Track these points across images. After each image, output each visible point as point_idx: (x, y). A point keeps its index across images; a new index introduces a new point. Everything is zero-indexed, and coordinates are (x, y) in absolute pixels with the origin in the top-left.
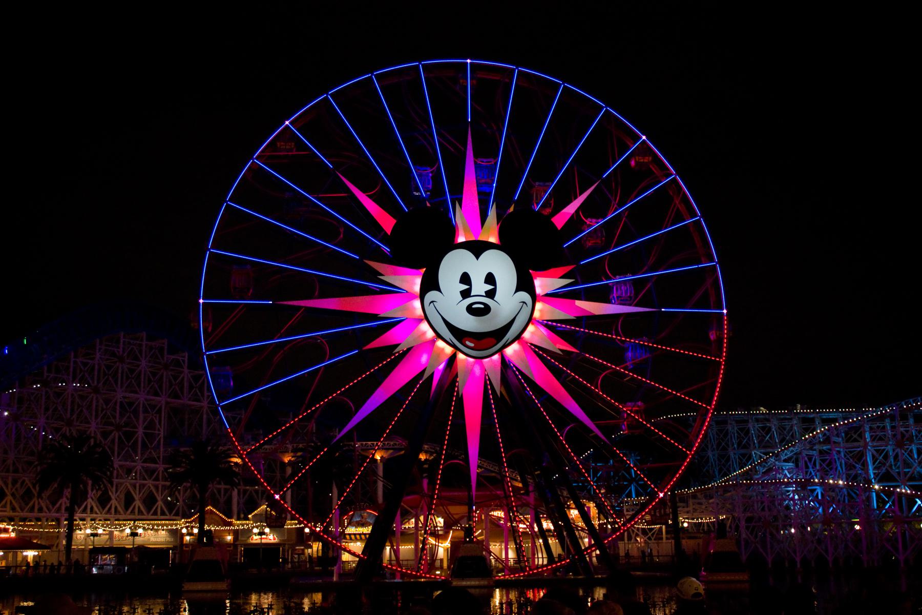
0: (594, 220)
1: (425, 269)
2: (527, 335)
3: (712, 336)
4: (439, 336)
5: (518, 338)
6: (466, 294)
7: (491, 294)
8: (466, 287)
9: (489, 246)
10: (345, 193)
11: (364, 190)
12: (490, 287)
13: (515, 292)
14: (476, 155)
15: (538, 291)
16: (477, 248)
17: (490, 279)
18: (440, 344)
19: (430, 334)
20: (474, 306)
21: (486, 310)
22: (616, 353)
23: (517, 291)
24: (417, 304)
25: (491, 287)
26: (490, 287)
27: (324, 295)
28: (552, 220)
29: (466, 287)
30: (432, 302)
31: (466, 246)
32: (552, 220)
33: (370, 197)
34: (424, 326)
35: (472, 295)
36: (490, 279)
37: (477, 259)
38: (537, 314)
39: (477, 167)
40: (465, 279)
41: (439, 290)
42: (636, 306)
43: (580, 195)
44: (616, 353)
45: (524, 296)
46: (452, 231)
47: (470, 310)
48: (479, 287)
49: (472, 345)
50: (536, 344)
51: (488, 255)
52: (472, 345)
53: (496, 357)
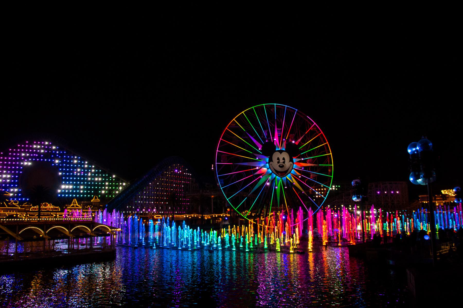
0: (304, 143)
1: (269, 157)
2: (292, 172)
3: (329, 171)
4: (273, 172)
5: (290, 173)
6: (278, 162)
7: (284, 162)
8: (278, 161)
9: (283, 151)
10: (247, 136)
11: (252, 136)
12: (284, 161)
14: (278, 127)
15: (294, 161)
16: (281, 152)
18: (273, 173)
19: (271, 172)
20: (281, 165)
22: (308, 175)
23: (290, 161)
24: (268, 165)
26: (284, 161)
27: (243, 162)
28: (297, 144)
29: (278, 161)
30: (271, 164)
31: (278, 151)
32: (297, 144)
33: (254, 138)
34: (269, 170)
35: (280, 162)
36: (284, 159)
37: (281, 153)
38: (294, 167)
39: (278, 130)
41: (273, 162)
42: (314, 164)
43: (301, 137)
44: (308, 175)
45: (291, 163)
46: (275, 148)
47: (279, 166)
49: (280, 174)
50: (293, 174)
51: (283, 153)
52: (280, 174)
53: (285, 177)
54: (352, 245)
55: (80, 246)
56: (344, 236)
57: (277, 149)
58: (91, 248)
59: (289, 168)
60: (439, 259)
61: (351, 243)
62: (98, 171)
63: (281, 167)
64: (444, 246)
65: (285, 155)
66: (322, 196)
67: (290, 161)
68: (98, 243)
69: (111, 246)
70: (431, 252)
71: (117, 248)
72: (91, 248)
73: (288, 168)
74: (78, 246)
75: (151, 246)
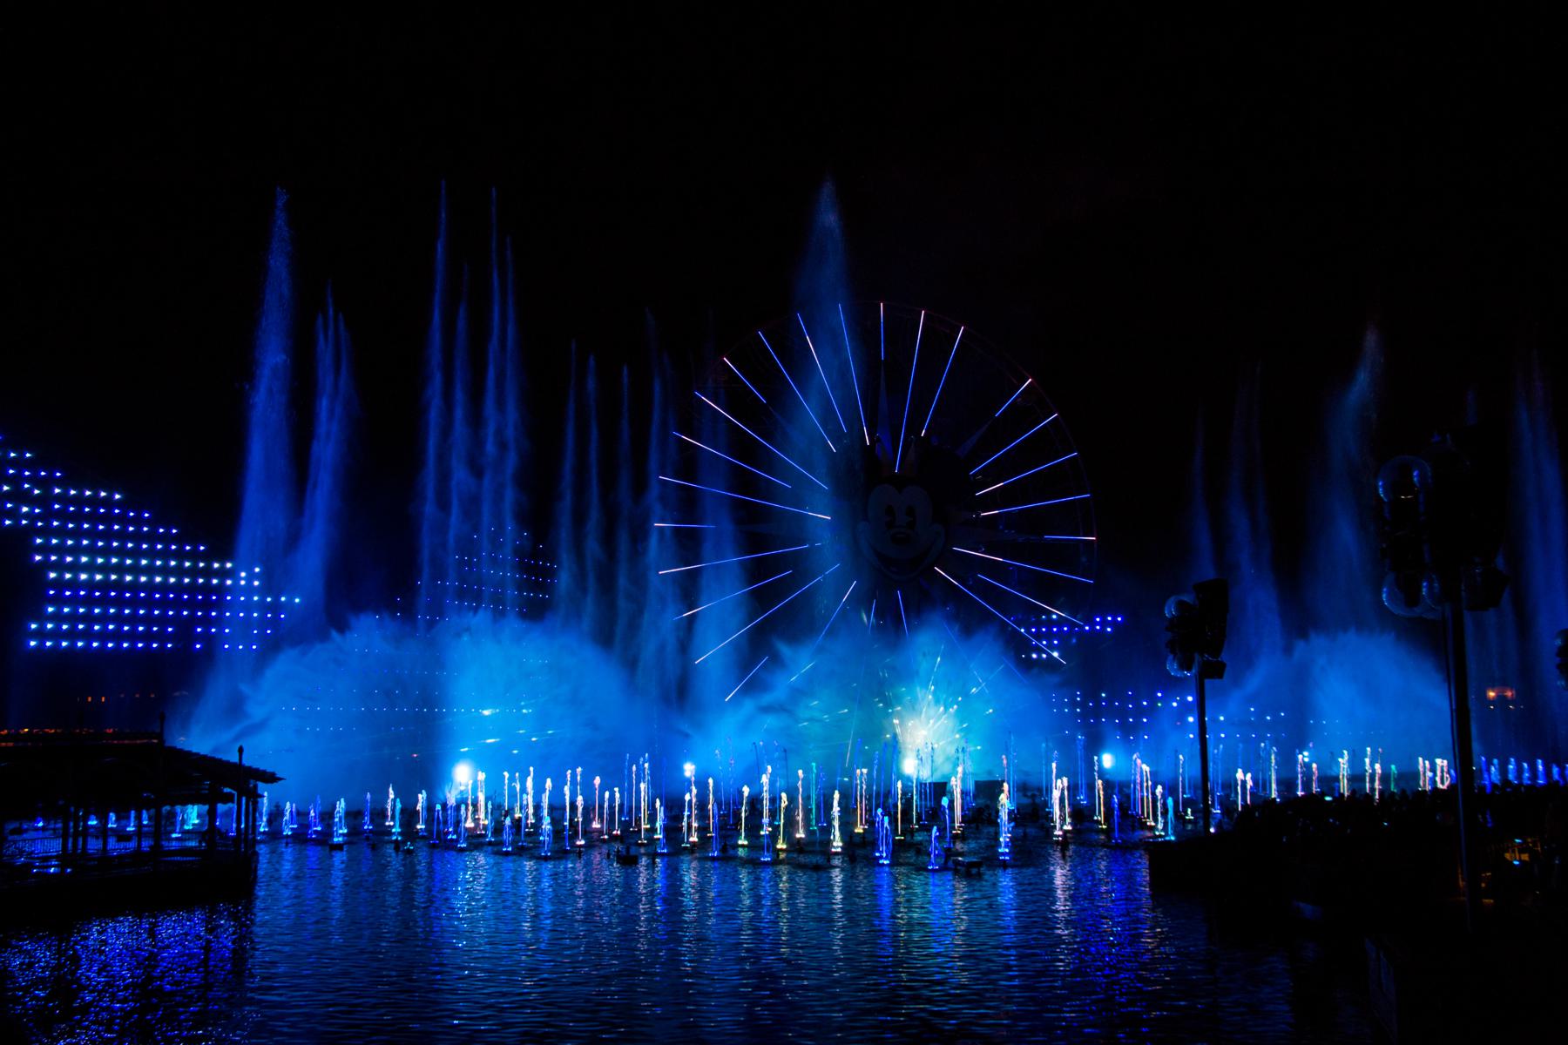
54: (1162, 842)
55: (112, 843)
56: (1132, 808)
58: (157, 848)
60: (1492, 901)
61: (1160, 836)
62: (195, 549)
64: (1514, 852)
66: (1055, 654)
68: (186, 827)
69: (236, 840)
70: (1460, 876)
71: (262, 850)
72: (157, 848)
74: (105, 844)
75: (397, 839)
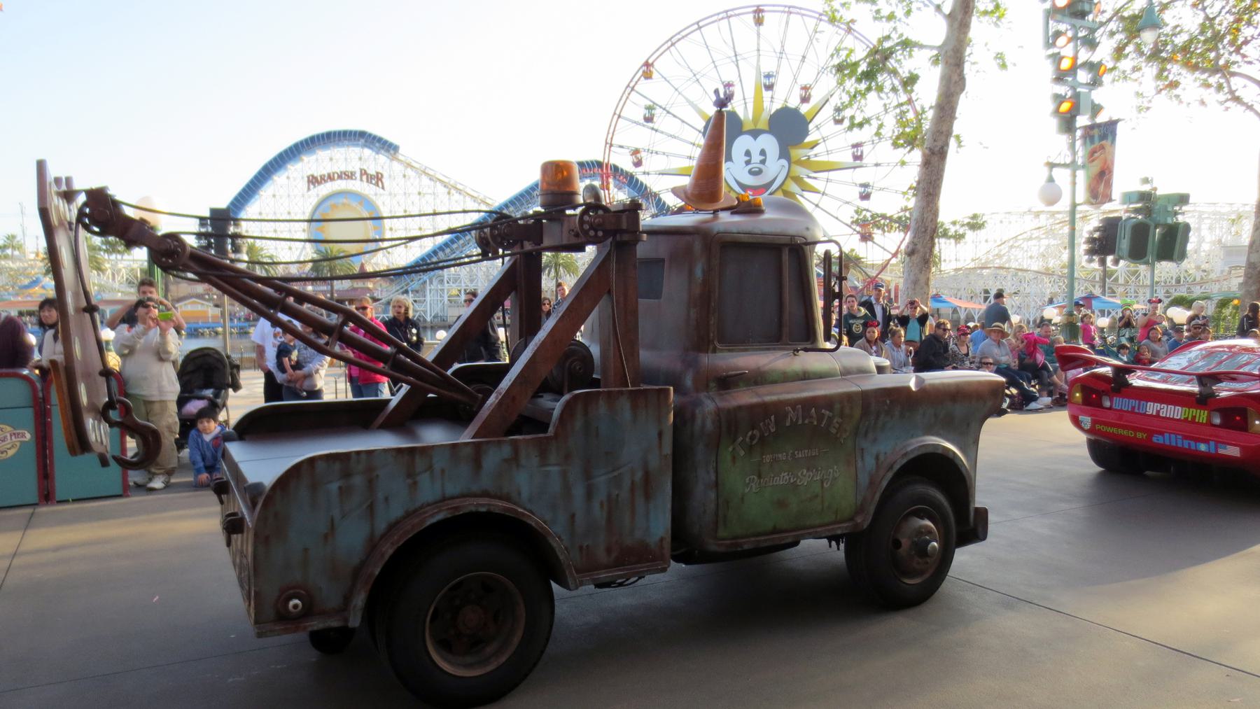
6: (748, 163)
7: (763, 162)
8: (748, 158)
12: (764, 157)
13: (779, 159)
16: (755, 134)
17: (763, 153)
20: (753, 170)
21: (760, 172)
25: (764, 157)
26: (763, 158)
29: (748, 158)
35: (752, 162)
36: (763, 153)
37: (755, 139)
40: (748, 153)
45: (784, 162)
47: (751, 172)
48: (756, 158)
57: (746, 128)
59: (777, 176)
63: (756, 173)
65: (769, 143)
67: (780, 158)
73: (774, 177)
